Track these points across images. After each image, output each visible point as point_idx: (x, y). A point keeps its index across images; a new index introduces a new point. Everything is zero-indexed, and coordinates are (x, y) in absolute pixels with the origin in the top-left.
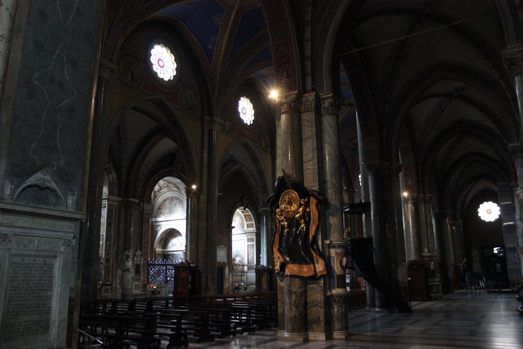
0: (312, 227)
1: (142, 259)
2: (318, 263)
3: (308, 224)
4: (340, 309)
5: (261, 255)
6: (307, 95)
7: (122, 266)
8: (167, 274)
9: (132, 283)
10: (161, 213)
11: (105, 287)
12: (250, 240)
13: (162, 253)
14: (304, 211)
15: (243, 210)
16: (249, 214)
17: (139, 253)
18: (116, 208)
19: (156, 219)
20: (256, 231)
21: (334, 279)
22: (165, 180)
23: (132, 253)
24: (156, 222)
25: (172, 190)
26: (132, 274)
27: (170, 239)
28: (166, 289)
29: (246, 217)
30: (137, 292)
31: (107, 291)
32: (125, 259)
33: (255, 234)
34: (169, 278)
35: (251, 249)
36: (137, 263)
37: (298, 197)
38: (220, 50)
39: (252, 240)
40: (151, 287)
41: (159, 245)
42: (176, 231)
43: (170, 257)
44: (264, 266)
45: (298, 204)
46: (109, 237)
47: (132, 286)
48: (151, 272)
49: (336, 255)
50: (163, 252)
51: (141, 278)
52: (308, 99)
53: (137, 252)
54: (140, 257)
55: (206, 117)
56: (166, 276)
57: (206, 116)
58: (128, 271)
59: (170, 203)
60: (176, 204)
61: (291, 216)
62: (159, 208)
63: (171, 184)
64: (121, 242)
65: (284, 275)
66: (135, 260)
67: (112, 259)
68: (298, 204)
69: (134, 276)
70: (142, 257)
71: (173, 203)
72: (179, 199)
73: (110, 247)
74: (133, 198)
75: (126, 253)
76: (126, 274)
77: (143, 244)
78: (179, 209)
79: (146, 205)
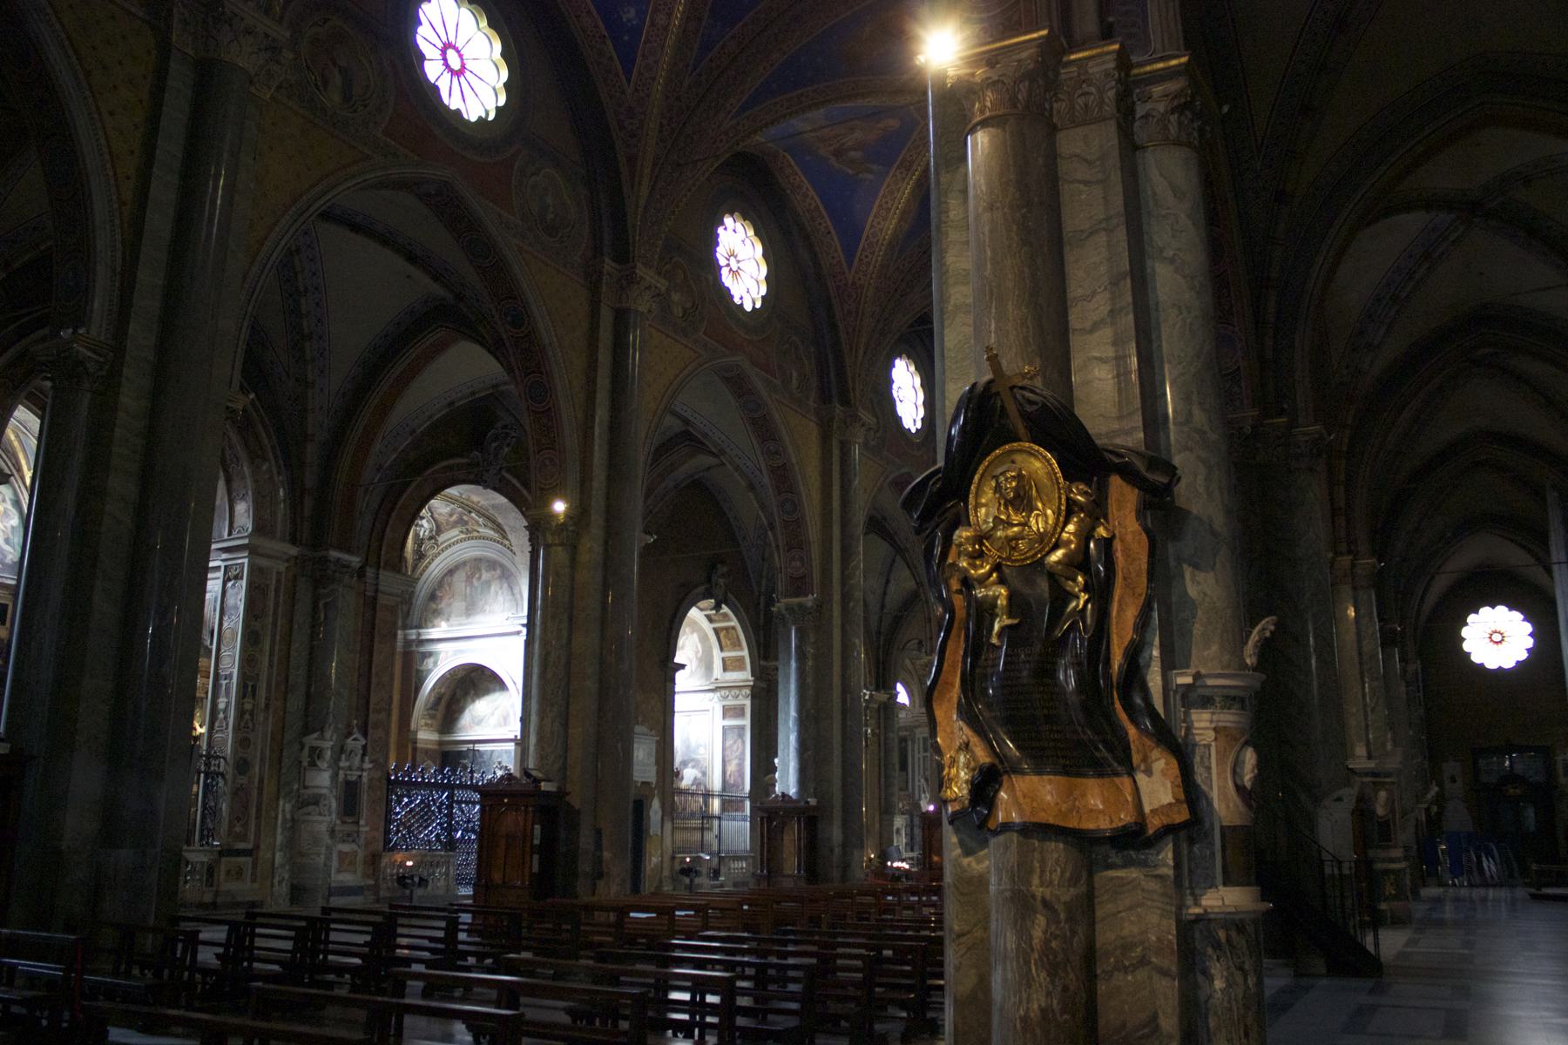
0: (1120, 610)
1: (367, 765)
2: (1149, 772)
3: (1101, 592)
4: (1239, 977)
5: (776, 761)
6: (1080, 55)
7: (296, 787)
8: (453, 819)
9: (328, 848)
10: (437, 613)
11: (233, 859)
12: (731, 713)
13: (436, 747)
14: (1085, 535)
15: (711, 609)
16: (732, 624)
17: (356, 742)
18: (278, 581)
19: (421, 631)
20: (752, 683)
21: (1212, 844)
22: (451, 500)
23: (331, 740)
24: (422, 642)
25: (476, 534)
26: (330, 815)
27: (465, 701)
28: (448, 868)
29: (722, 635)
30: (347, 878)
31: (240, 873)
32: (305, 764)
33: (748, 692)
34: (460, 832)
35: (735, 742)
36: (349, 778)
37: (1059, 475)
38: (666, 29)
39: (736, 712)
40: (396, 861)
41: (429, 722)
42: (487, 673)
43: (465, 761)
44: (788, 796)
45: (1060, 504)
46: (250, 684)
47: (328, 858)
48: (398, 810)
49: (1216, 739)
50: (441, 743)
51: (361, 829)
52: (1087, 72)
53: (349, 741)
54: (359, 756)
55: (609, 265)
56: (450, 824)
57: (607, 260)
58: (316, 803)
59: (469, 579)
60: (488, 583)
61: (1027, 558)
62: (433, 597)
63: (473, 515)
64: (296, 702)
65: (992, 825)
66: (343, 768)
67: (258, 759)
68: (1060, 504)
69: (338, 822)
70: (367, 758)
71: (479, 578)
72: (502, 566)
73: (252, 720)
74: (340, 548)
75: (311, 740)
76: (309, 814)
77: (371, 710)
78: (501, 598)
79: (385, 575)
